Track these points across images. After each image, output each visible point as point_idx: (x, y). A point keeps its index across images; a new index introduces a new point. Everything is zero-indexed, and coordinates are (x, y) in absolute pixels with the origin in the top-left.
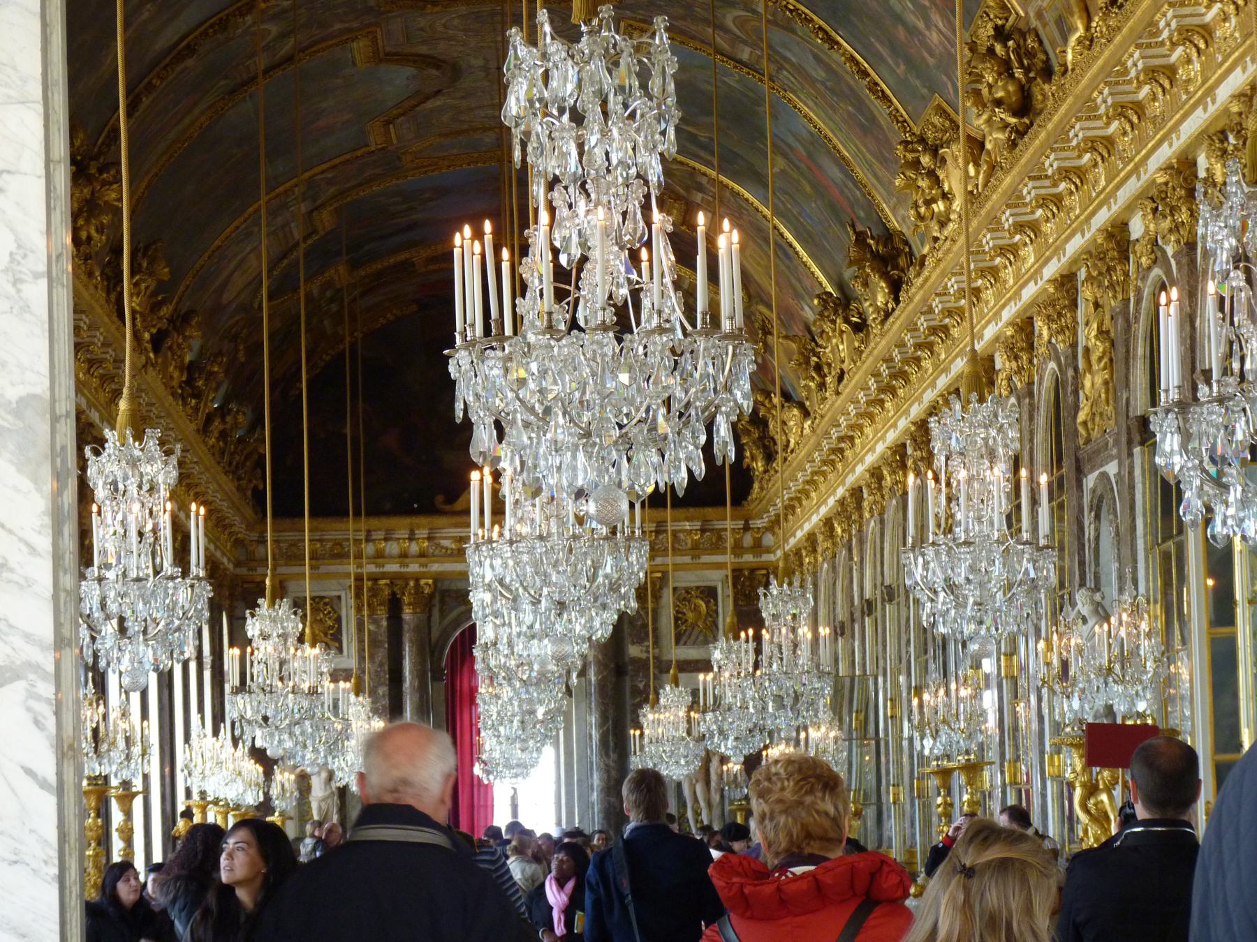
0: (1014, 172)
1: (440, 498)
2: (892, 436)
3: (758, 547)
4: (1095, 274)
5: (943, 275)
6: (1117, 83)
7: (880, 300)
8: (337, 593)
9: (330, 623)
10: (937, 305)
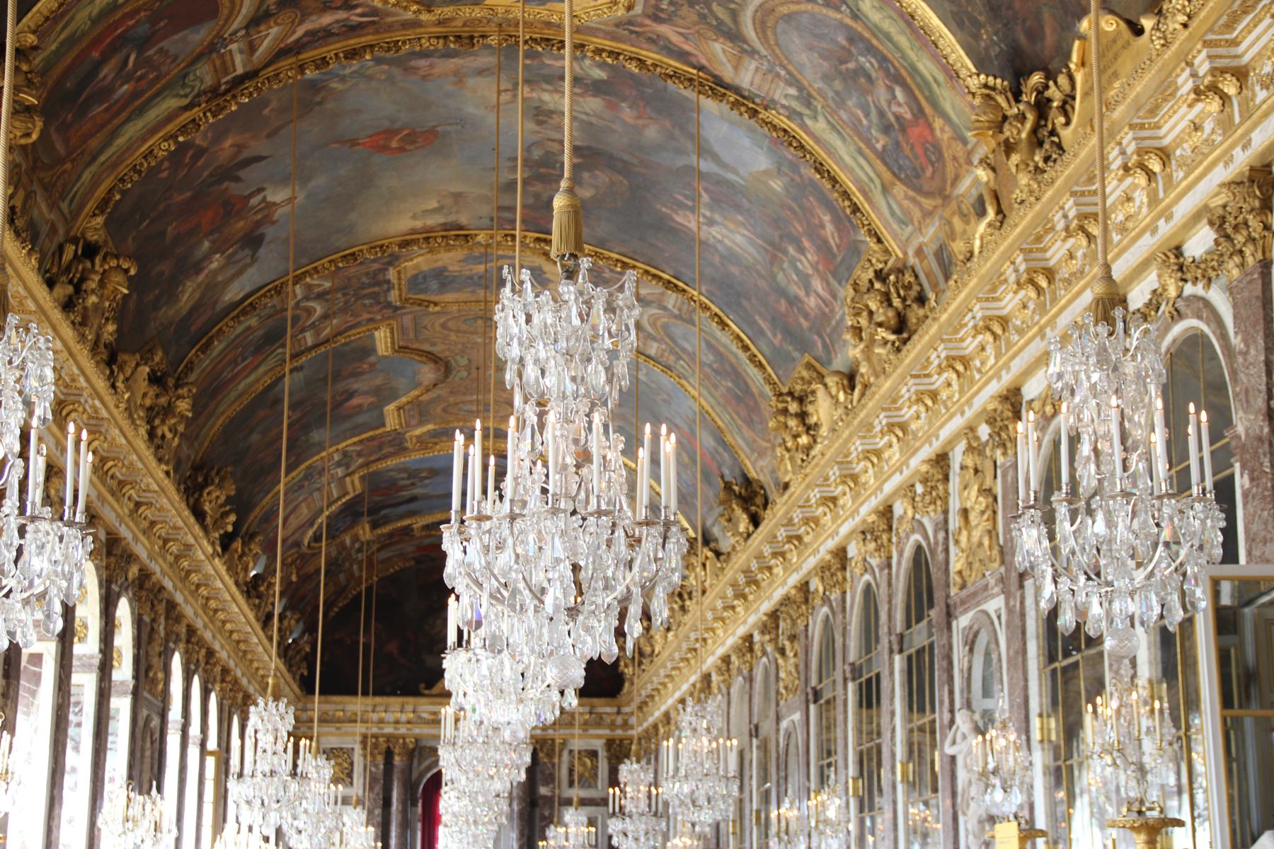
0: (895, 375)
1: (422, 685)
2: (742, 631)
3: (626, 725)
4: (975, 444)
5: (808, 487)
6: (1031, 251)
7: (742, 528)
8: (350, 746)
9: (346, 765)
10: (797, 516)
